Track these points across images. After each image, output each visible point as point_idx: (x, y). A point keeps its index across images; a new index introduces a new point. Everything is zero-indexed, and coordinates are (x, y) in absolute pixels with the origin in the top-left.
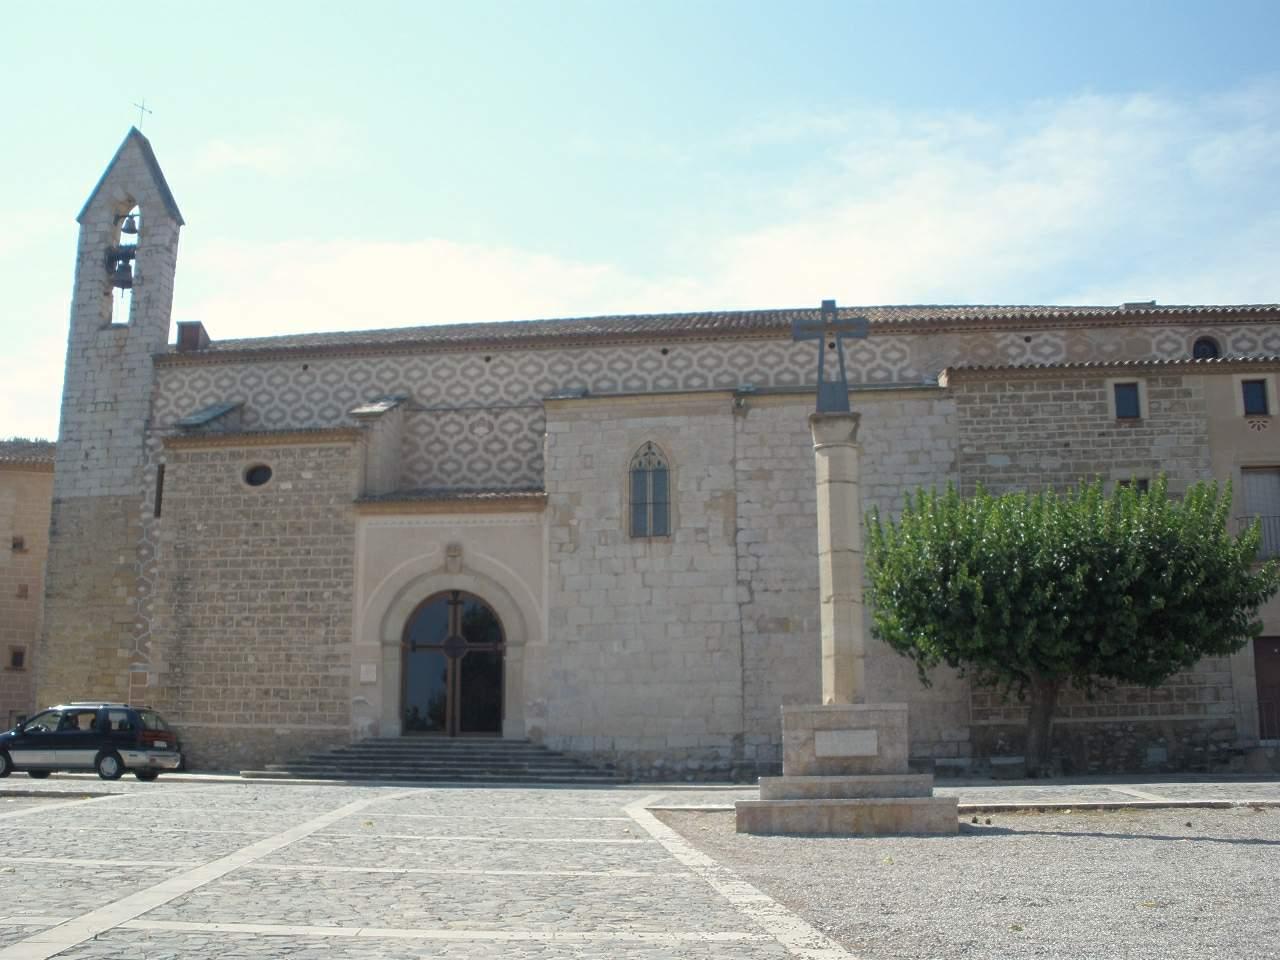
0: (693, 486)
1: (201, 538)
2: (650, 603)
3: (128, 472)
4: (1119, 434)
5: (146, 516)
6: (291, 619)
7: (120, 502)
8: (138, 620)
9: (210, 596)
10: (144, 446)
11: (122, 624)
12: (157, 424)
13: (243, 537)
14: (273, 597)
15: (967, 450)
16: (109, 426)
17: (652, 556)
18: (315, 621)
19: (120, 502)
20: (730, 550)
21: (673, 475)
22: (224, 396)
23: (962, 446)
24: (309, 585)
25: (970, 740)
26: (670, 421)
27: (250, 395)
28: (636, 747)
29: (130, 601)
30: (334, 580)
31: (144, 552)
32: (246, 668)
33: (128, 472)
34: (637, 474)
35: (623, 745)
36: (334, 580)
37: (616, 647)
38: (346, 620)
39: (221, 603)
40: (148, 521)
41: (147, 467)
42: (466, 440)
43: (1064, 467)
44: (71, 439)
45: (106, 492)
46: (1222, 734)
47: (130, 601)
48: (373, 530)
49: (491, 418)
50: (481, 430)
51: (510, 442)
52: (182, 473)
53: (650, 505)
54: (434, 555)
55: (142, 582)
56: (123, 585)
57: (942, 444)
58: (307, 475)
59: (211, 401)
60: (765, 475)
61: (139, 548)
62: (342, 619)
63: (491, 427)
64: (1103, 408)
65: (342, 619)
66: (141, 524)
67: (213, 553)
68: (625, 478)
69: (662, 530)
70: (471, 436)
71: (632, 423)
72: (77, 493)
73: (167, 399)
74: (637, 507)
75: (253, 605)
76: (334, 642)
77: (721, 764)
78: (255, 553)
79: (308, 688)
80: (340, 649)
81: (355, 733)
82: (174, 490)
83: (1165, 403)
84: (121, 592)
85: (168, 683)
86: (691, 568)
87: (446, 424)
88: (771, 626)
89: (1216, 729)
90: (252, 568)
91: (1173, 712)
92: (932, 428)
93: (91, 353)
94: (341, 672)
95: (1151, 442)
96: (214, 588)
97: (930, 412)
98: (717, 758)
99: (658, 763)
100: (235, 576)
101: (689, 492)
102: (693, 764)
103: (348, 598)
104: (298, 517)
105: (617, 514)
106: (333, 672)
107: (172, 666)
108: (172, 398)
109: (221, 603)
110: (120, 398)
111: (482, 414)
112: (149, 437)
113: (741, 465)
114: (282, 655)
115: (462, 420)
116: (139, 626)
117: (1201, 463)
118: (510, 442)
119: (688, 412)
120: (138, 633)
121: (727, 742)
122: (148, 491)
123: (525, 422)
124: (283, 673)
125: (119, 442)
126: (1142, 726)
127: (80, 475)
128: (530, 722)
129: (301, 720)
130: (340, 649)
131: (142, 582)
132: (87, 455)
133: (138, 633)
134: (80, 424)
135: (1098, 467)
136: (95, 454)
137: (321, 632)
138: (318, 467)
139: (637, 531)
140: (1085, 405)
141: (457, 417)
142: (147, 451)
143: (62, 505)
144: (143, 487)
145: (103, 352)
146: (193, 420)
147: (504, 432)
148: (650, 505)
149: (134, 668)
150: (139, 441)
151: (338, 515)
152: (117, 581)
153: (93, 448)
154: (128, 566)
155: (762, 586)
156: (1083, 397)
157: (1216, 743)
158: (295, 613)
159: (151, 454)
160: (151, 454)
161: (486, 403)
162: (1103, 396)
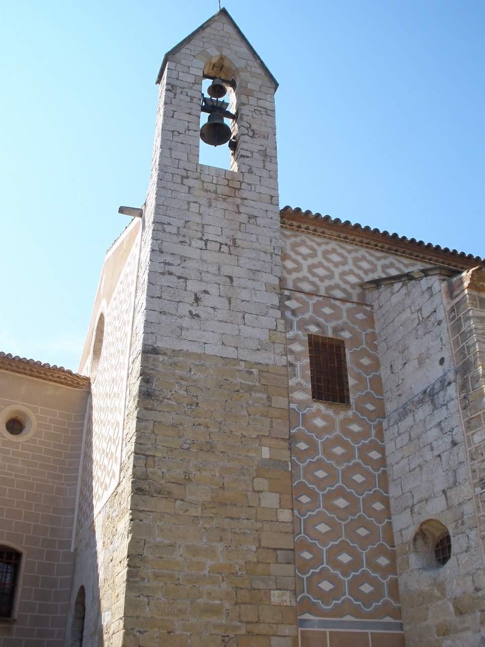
5: (299, 396)
11: (275, 549)
16: (226, 270)
19: (255, 371)
33: (265, 336)
41: (290, 334)
44: (170, 274)
45: (231, 353)
47: (285, 515)
56: (271, 491)
66: (292, 406)
72: (185, 346)
84: (270, 500)
93: (190, 182)
110: (238, 242)
112: (289, 298)
116: (307, 555)
122: (298, 364)
125: (244, 295)
127: (187, 322)
131: (303, 489)
132: (197, 299)
133: (304, 566)
134: (184, 259)
136: (207, 300)
142: (288, 314)
143: (161, 358)
144: (291, 358)
149: (302, 623)
150: (276, 301)
152: (261, 483)
153: (206, 292)
154: (273, 463)
160: (295, 320)
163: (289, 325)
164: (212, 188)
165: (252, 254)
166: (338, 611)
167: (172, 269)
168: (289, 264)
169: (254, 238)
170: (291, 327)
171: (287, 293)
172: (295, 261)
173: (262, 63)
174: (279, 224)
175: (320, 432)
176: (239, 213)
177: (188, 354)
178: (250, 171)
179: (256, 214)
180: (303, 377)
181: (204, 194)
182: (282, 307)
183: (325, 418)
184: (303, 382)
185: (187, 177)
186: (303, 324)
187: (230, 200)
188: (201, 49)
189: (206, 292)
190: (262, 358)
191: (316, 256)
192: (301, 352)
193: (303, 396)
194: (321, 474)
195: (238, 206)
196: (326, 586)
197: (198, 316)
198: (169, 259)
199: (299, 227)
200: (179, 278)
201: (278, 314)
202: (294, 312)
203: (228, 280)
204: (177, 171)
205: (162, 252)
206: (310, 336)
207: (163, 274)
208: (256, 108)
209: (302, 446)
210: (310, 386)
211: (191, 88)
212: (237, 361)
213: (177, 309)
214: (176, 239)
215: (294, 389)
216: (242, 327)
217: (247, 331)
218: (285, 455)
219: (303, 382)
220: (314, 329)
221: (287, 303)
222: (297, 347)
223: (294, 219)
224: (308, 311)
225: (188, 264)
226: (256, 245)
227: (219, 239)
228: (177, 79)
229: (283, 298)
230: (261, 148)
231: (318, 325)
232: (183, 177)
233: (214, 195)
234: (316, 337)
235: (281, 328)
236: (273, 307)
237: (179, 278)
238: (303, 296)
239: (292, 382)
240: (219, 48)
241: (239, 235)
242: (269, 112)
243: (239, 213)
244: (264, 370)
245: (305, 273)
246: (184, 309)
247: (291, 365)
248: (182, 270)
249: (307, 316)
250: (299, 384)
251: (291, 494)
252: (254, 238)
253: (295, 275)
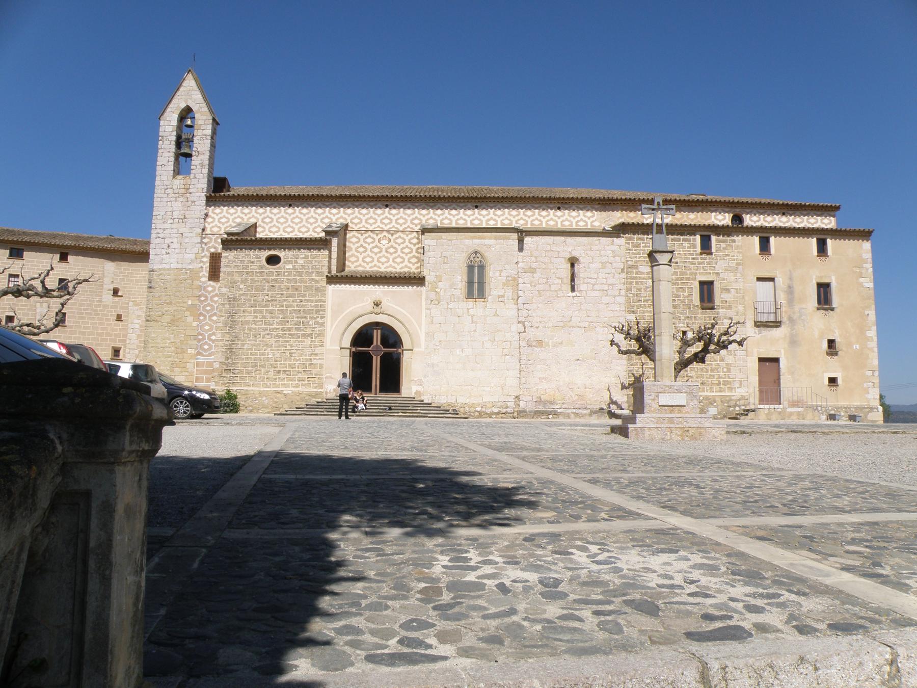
0: (497, 274)
1: (241, 292)
2: (475, 331)
4: (702, 259)
5: (203, 279)
6: (291, 335)
8: (199, 334)
9: (247, 323)
10: (202, 242)
12: (208, 231)
13: (266, 292)
14: (281, 323)
15: (629, 263)
16: (181, 231)
17: (476, 308)
18: (304, 336)
20: (515, 307)
21: (487, 269)
22: (246, 218)
23: (627, 261)
24: (302, 317)
25: (627, 402)
26: (487, 242)
27: (260, 218)
28: (467, 401)
29: (195, 324)
30: (315, 315)
31: (203, 299)
32: (268, 359)
33: (193, 256)
34: (470, 268)
35: (461, 400)
36: (315, 315)
37: (458, 352)
38: (321, 335)
39: (254, 326)
40: (204, 282)
42: (376, 246)
43: (675, 273)
45: (180, 266)
46: (742, 402)
47: (195, 324)
48: (333, 290)
49: (390, 236)
50: (384, 242)
51: (399, 248)
52: (231, 258)
53: (476, 282)
54: (368, 305)
55: (201, 314)
57: (618, 259)
58: (301, 261)
59: (238, 220)
60: (532, 271)
61: (200, 296)
62: (319, 335)
63: (389, 240)
64: (695, 246)
65: (319, 335)
67: (249, 300)
68: (465, 270)
69: (482, 294)
70: (379, 245)
71: (467, 242)
73: (213, 218)
74: (470, 283)
75: (272, 327)
76: (315, 347)
77: (509, 410)
78: (272, 300)
79: (301, 370)
80: (318, 350)
81: (326, 393)
82: (227, 266)
83: (723, 245)
85: (225, 367)
86: (496, 315)
87: (366, 238)
88: (534, 344)
89: (739, 400)
90: (271, 308)
91: (721, 391)
92: (613, 251)
94: (319, 362)
95: (716, 263)
96: (250, 318)
97: (613, 243)
98: (507, 407)
99: (479, 409)
100: (261, 312)
101: (494, 277)
102: (496, 410)
103: (322, 324)
104: (296, 282)
105: (459, 287)
106: (314, 362)
107: (227, 358)
108: (217, 218)
109: (254, 326)
111: (385, 233)
113: (520, 265)
114: (287, 353)
115: (374, 236)
116: (200, 337)
117: (739, 275)
118: (399, 248)
119: (496, 238)
120: (199, 341)
121: (512, 399)
123: (407, 239)
124: (288, 362)
126: (707, 398)
128: (415, 389)
129: (297, 387)
130: (318, 350)
131: (201, 314)
133: (199, 341)
134: (164, 230)
135: (691, 274)
137: (308, 341)
138: (306, 257)
139: (470, 295)
140: (686, 244)
141: (372, 235)
145: (176, 191)
146: (235, 230)
147: (396, 243)
148: (476, 282)
151: (317, 282)
152: (187, 313)
155: (530, 325)
156: (685, 240)
157: (739, 406)
158: (294, 332)
159: (206, 247)
160: (206, 247)
161: (386, 228)
162: (695, 240)
163: (203, 250)
166: (210, 355)
175: (210, 292)
177: (164, 269)
183: (212, 286)
186: (210, 248)
190: (191, 267)
193: (205, 279)
194: (208, 308)
196: (206, 347)
198: (158, 231)
202: (206, 244)
209: (203, 299)
212: (181, 269)
218: (197, 302)
220: (213, 250)
229: (203, 238)
246: (164, 251)
251: (197, 316)
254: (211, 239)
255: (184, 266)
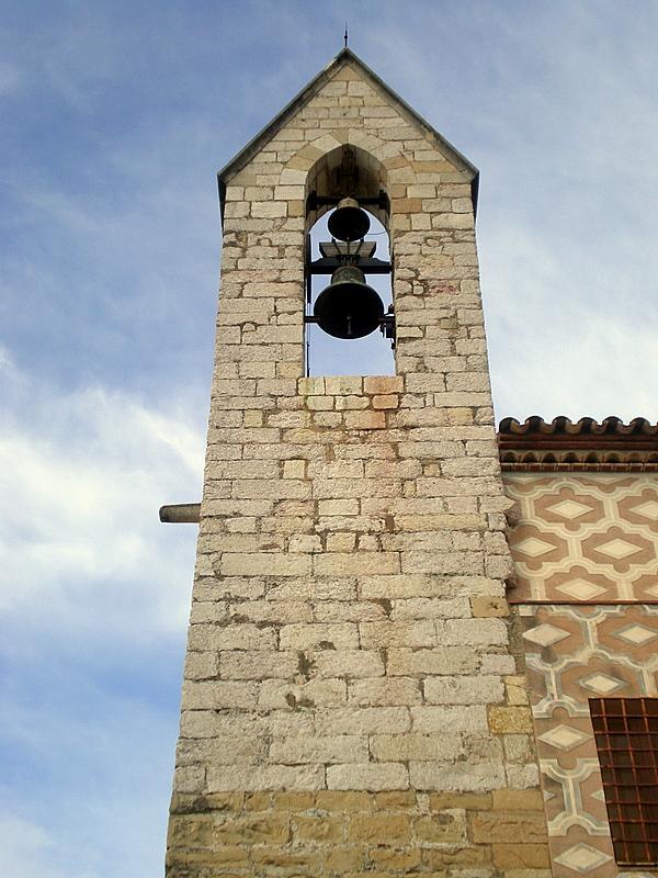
3: (475, 721)
7: (458, 813)
16: (373, 587)
33: (476, 721)
41: (542, 708)
44: (240, 620)
45: (394, 777)
72: (271, 778)
110: (399, 522)
112: (532, 622)
122: (569, 778)
125: (418, 634)
127: (279, 722)
132: (305, 666)
134: (272, 582)
136: (328, 663)
142: (534, 661)
143: (218, 818)
144: (547, 766)
150: (499, 633)
153: (327, 645)
160: (552, 672)
163: (537, 685)
164: (332, 419)
165: (430, 541)
167: (242, 609)
168: (533, 547)
169: (436, 505)
170: (543, 689)
171: (525, 611)
172: (549, 538)
173: (437, 136)
174: (496, 463)
176: (399, 459)
177: (281, 796)
178: (422, 367)
179: (438, 451)
180: (587, 806)
181: (317, 436)
182: (516, 646)
184: (588, 823)
185: (277, 410)
187: (374, 437)
188: (300, 145)
189: (327, 645)
190: (473, 779)
191: (604, 516)
192: (575, 750)
195: (395, 446)
197: (308, 703)
198: (236, 588)
199: (550, 459)
200: (262, 625)
201: (509, 663)
202: (548, 654)
203: (379, 609)
204: (253, 403)
205: (220, 577)
206: (594, 704)
207: (223, 624)
208: (430, 233)
210: (606, 829)
211: (279, 229)
212: (406, 797)
213: (256, 696)
214: (252, 543)
215: (562, 843)
216: (417, 709)
217: (428, 718)
219: (588, 823)
220: (603, 686)
221: (529, 635)
222: (562, 737)
223: (534, 447)
224: (583, 644)
225: (284, 591)
226: (445, 519)
227: (355, 525)
228: (249, 217)
229: (514, 625)
230: (444, 313)
231: (613, 672)
232: (267, 413)
233: (338, 435)
234: (612, 703)
235: (518, 696)
236: (494, 649)
237: (262, 625)
238: (570, 612)
239: (555, 827)
240: (334, 131)
241: (399, 507)
242: (459, 236)
243: (399, 459)
244: (476, 804)
245: (575, 557)
246: (273, 694)
247: (551, 782)
248: (267, 607)
249: (582, 657)
250: (576, 828)
252: (436, 505)
253: (549, 569)
254: (576, 630)
255: (423, 776)
